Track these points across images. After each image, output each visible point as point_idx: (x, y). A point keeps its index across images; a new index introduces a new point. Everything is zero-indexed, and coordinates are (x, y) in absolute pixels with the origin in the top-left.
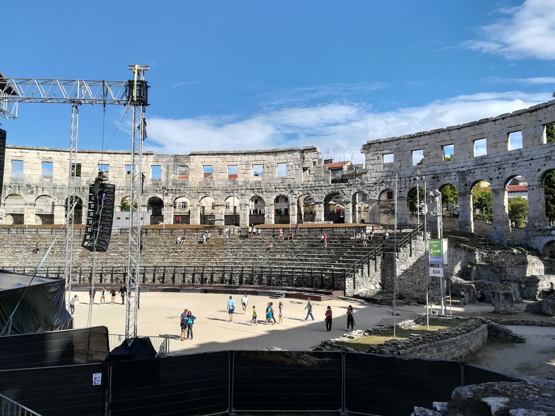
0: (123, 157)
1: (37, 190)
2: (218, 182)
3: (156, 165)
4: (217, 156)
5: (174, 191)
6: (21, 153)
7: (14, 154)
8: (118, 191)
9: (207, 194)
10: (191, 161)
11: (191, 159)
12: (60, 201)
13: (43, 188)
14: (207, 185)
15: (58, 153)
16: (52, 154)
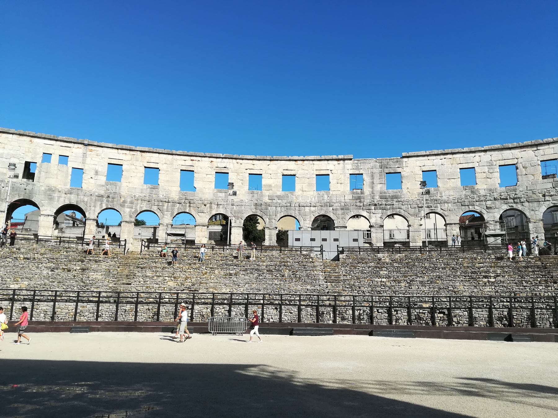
0: (313, 165)
1: (211, 207)
2: (447, 192)
3: (356, 173)
4: (442, 157)
5: (384, 206)
6: (192, 161)
7: (183, 163)
8: (309, 208)
9: (432, 208)
10: (404, 165)
11: (404, 163)
12: (238, 221)
13: (218, 205)
14: (431, 197)
15: (234, 160)
16: (227, 162)
